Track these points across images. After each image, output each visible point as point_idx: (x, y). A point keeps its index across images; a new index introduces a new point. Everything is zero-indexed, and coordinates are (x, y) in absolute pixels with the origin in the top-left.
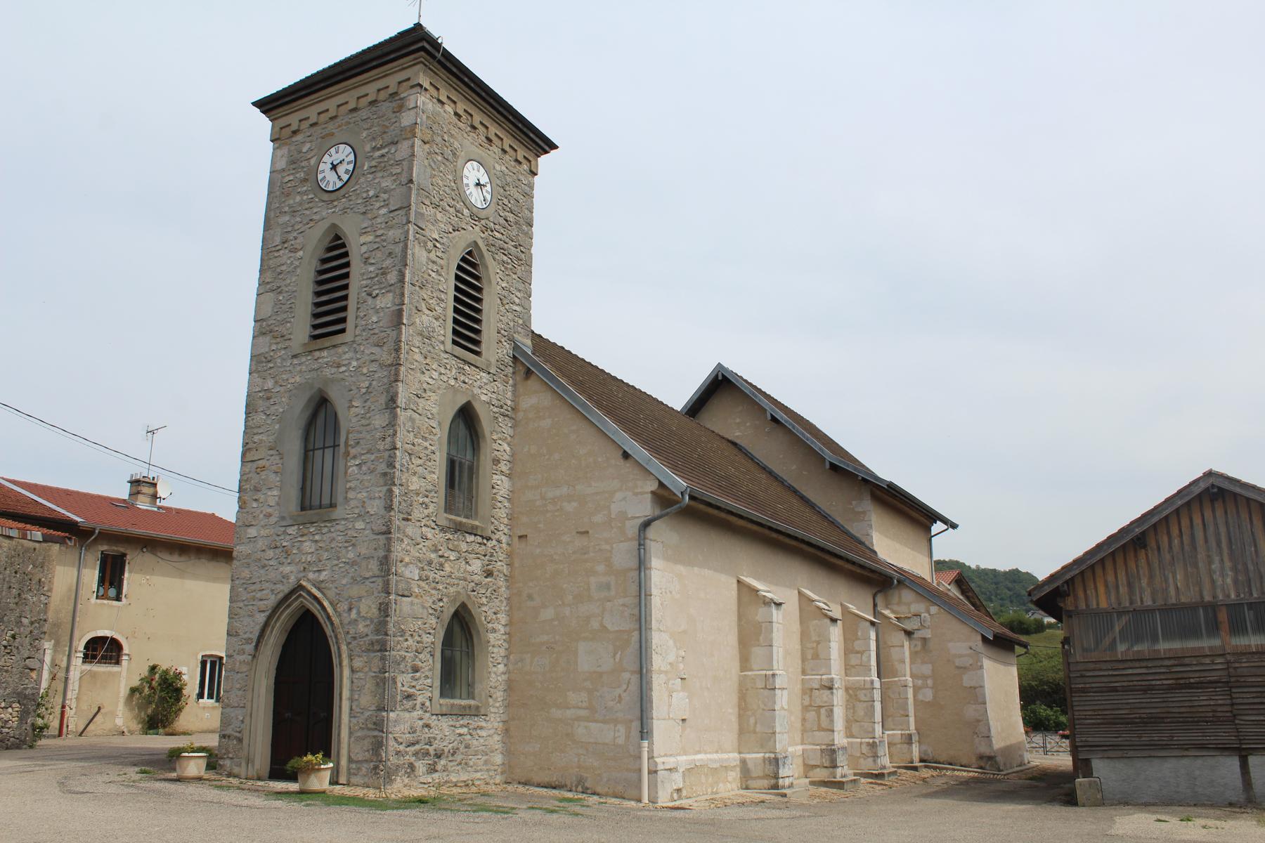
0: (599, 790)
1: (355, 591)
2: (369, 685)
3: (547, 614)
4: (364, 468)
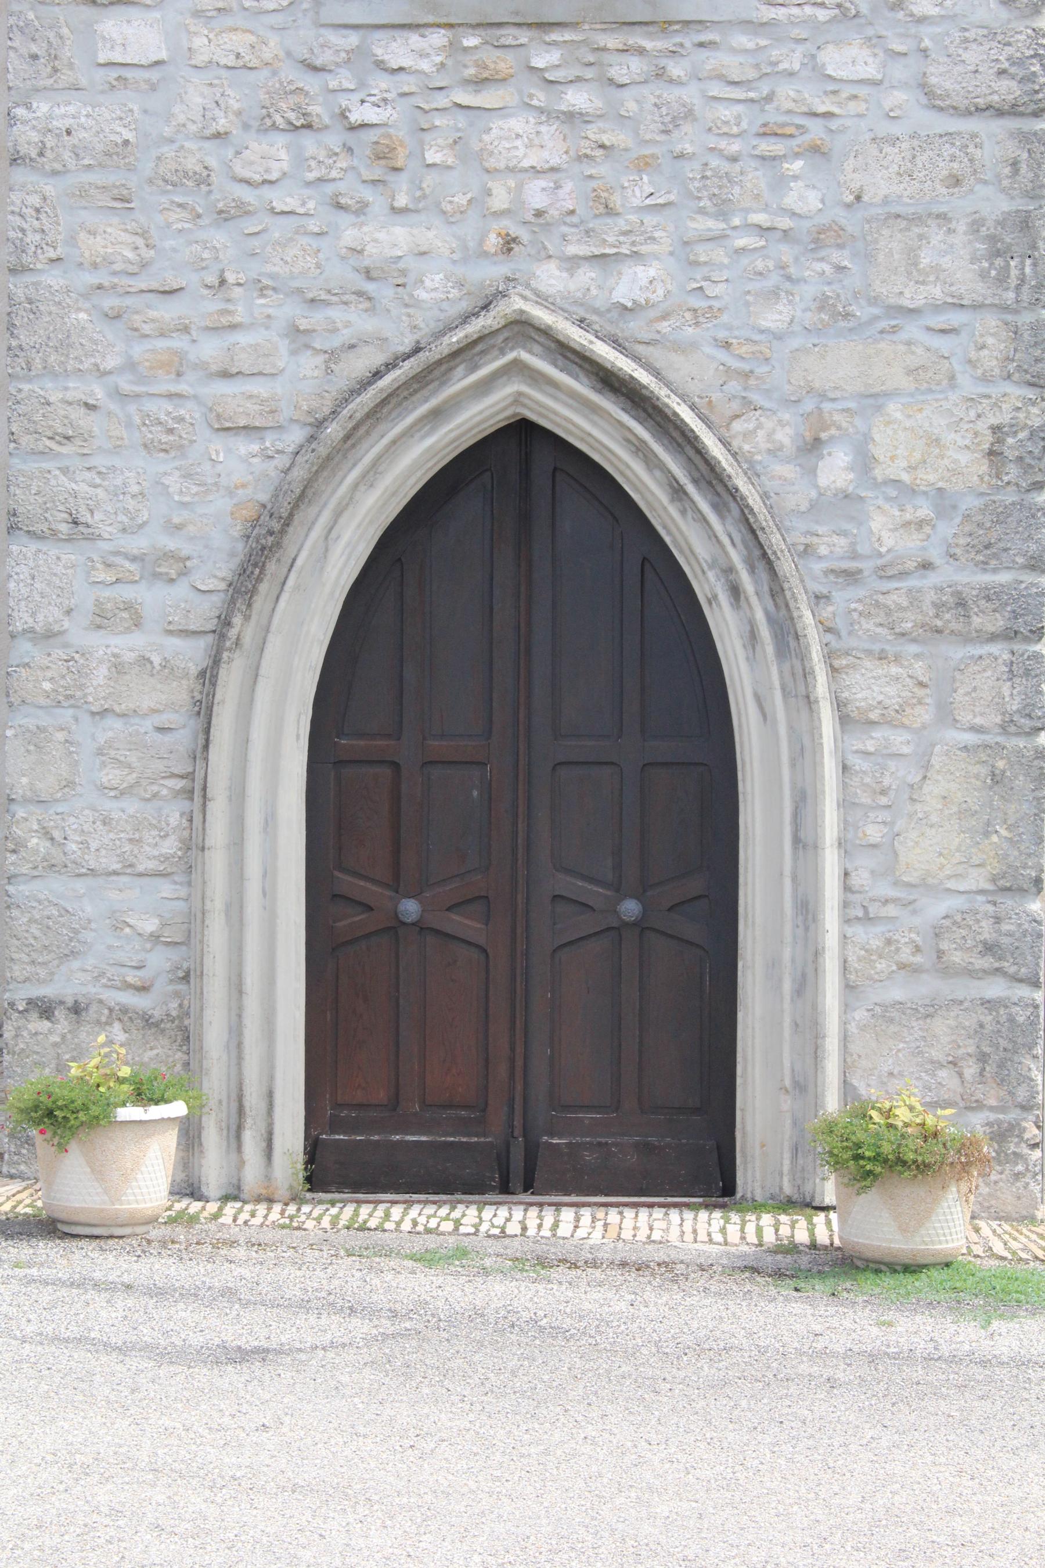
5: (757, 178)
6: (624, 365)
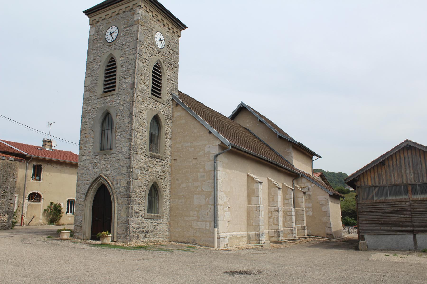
0: (200, 244)
1: (119, 178)
2: (124, 209)
3: (183, 185)
4: (122, 136)
5: (115, 164)
6: (107, 179)
